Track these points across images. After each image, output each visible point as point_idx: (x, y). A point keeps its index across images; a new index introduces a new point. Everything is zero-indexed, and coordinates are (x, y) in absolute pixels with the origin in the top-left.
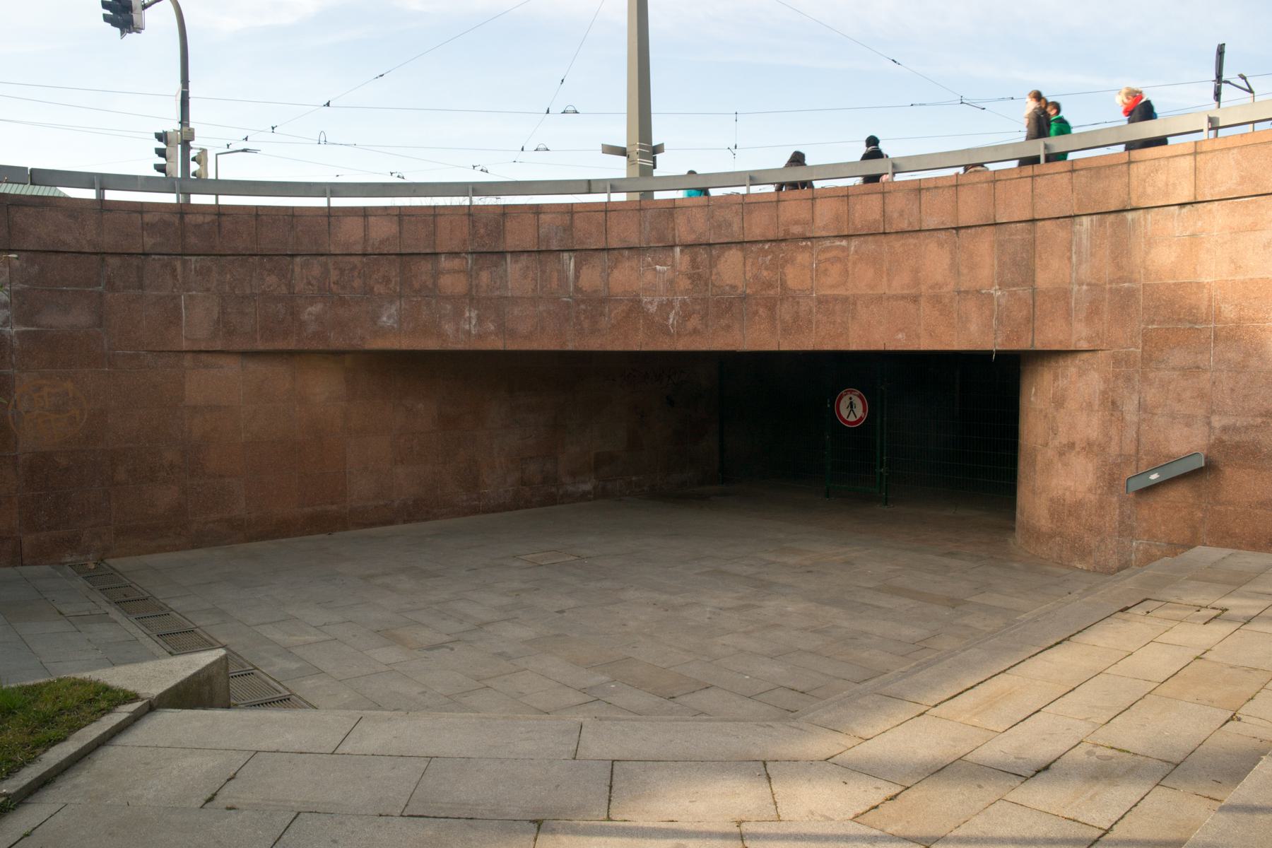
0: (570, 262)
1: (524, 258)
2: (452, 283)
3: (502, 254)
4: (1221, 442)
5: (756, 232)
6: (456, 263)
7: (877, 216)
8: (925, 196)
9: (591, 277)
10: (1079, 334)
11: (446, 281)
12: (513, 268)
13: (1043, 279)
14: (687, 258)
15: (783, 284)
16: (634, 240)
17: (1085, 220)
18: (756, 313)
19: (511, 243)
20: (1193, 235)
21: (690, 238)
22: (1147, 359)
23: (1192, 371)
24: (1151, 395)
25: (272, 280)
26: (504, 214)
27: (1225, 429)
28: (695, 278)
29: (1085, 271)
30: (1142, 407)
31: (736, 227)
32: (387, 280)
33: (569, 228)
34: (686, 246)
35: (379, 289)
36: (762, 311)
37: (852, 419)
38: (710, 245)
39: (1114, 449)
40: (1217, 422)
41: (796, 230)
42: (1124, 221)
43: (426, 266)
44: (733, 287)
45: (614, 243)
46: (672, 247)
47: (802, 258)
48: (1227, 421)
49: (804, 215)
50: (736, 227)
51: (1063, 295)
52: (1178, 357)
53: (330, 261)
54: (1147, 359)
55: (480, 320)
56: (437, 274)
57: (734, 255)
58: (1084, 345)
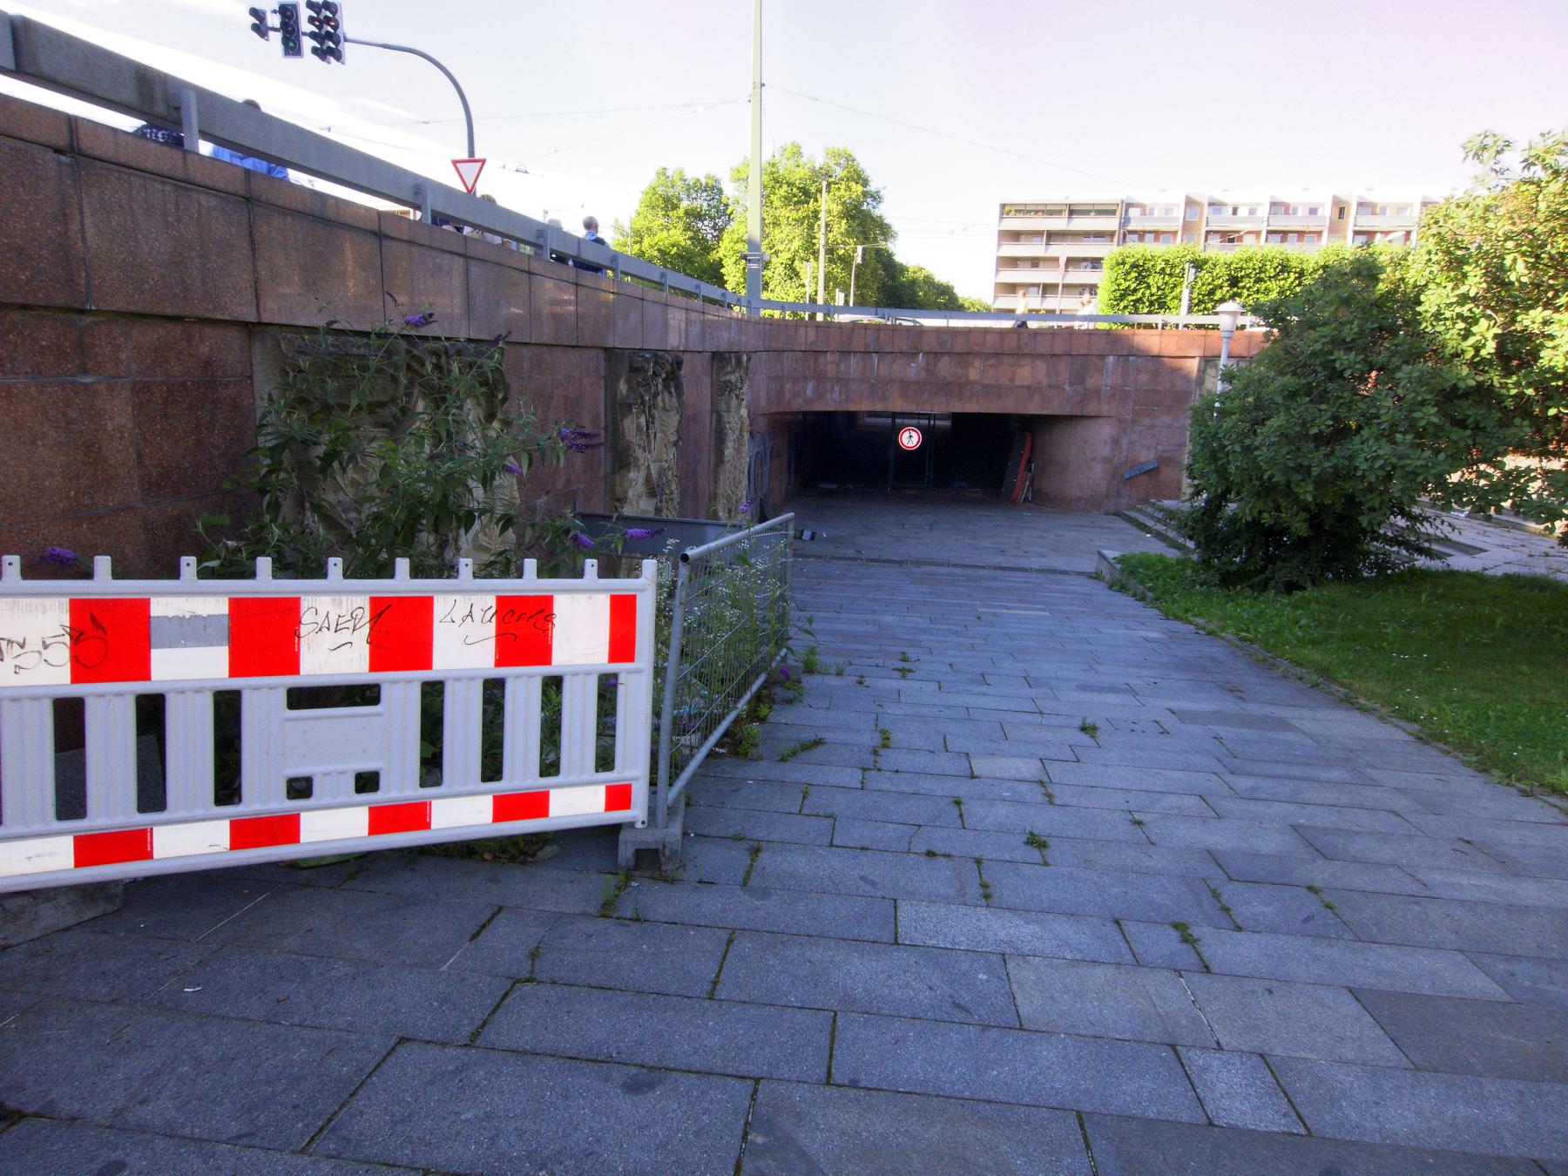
0: (875, 358)
1: (858, 355)
2: (831, 370)
3: (849, 352)
4: (1160, 456)
5: (958, 349)
7: (1015, 344)
8: (1038, 337)
10: (1105, 408)
11: (829, 367)
12: (853, 360)
13: (1090, 383)
14: (925, 360)
16: (904, 348)
19: (855, 347)
20: (1157, 370)
21: (928, 349)
22: (1133, 422)
23: (1151, 427)
24: (1134, 437)
26: (853, 329)
27: (1163, 451)
28: (927, 370)
29: (1109, 381)
30: (1130, 442)
31: (949, 344)
33: (878, 339)
34: (926, 353)
37: (910, 445)
38: (936, 353)
39: (1116, 460)
40: (1160, 448)
41: (977, 349)
42: (1128, 361)
45: (896, 350)
46: (917, 354)
47: (977, 363)
50: (949, 344)
51: (1098, 392)
52: (1147, 421)
54: (1133, 422)
55: (840, 393)
57: (945, 360)
58: (1105, 414)
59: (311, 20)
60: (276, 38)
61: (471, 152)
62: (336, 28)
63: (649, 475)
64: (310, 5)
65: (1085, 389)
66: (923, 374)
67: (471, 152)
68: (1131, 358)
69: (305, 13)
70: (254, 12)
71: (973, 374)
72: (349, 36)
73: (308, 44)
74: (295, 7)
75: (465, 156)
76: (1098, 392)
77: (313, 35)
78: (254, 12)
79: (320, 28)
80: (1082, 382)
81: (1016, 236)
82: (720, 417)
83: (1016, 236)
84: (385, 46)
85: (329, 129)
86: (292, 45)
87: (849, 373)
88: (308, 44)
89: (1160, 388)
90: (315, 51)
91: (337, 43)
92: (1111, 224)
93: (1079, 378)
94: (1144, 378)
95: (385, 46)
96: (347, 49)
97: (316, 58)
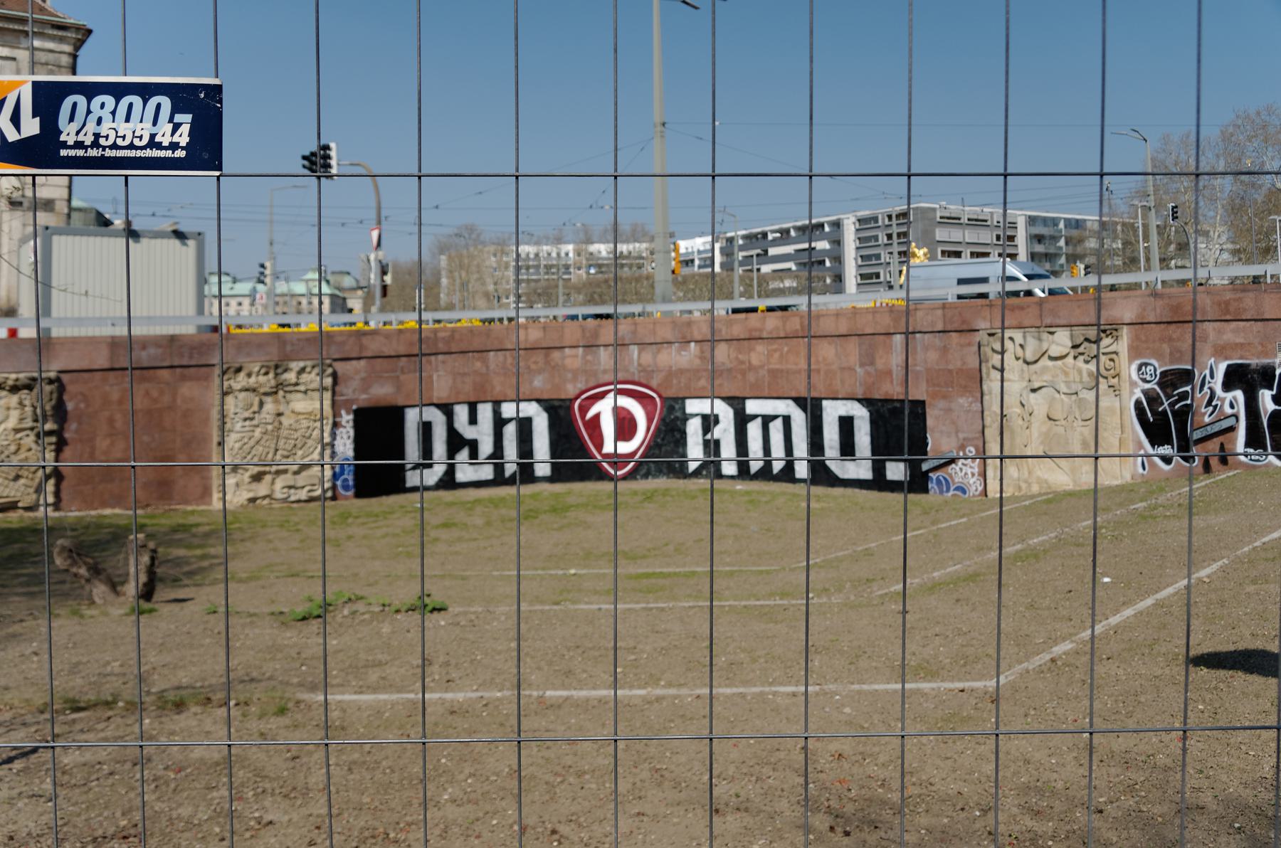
0: (635, 350)
6: (573, 351)
7: (798, 327)
9: (647, 358)
13: (880, 364)
14: (698, 348)
15: (750, 362)
17: (898, 336)
18: (735, 377)
19: (602, 341)
21: (699, 338)
25: (478, 364)
27: (964, 439)
31: (724, 333)
32: (536, 363)
34: (696, 342)
35: (533, 367)
36: (739, 376)
40: (961, 436)
43: (556, 355)
44: (723, 364)
46: (689, 342)
48: (965, 435)
49: (758, 325)
53: (508, 353)
56: (564, 358)
65: (876, 370)
66: (697, 362)
68: (918, 335)
71: (755, 359)
76: (889, 373)
80: (872, 363)
87: (599, 364)
89: (951, 367)
93: (868, 359)
94: (933, 356)
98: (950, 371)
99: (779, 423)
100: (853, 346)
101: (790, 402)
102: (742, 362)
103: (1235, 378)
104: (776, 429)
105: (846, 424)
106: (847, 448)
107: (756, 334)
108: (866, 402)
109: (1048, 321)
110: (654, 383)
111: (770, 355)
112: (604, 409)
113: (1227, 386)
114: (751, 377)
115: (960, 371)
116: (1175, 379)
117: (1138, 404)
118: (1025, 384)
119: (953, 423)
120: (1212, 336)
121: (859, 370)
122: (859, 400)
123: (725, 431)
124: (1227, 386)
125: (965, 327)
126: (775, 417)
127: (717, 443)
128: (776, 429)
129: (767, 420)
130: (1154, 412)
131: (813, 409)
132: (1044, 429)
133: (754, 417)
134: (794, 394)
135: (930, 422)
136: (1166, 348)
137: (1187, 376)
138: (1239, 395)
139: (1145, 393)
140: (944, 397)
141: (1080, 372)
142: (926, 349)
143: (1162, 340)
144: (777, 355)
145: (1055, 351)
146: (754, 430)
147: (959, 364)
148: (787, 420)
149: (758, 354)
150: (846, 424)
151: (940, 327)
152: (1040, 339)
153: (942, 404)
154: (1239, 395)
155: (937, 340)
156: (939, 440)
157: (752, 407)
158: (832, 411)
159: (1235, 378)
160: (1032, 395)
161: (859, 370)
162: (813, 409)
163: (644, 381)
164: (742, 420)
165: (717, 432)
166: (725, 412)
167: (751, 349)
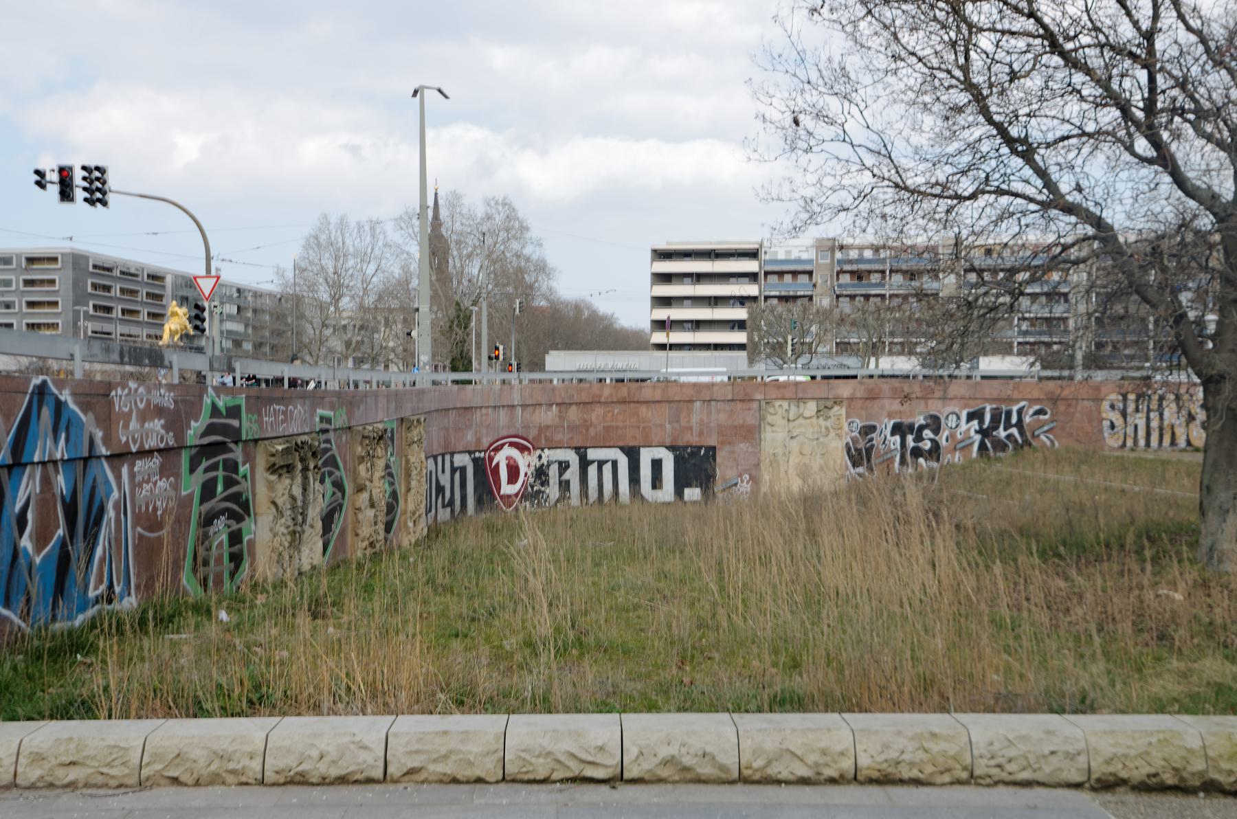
7: (626, 394)
21: (559, 401)
34: (557, 404)
57: (574, 408)
59: (84, 179)
60: (54, 190)
61: (208, 270)
62: (104, 183)
63: (371, 495)
64: (84, 168)
67: (208, 270)
69: (78, 175)
70: (37, 172)
72: (112, 188)
73: (80, 194)
74: (71, 169)
75: (203, 273)
76: (691, 428)
77: (85, 189)
78: (37, 172)
79: (91, 183)
80: (678, 421)
81: (666, 278)
82: (407, 461)
83: (666, 278)
84: (141, 196)
85: (71, 239)
86: (66, 194)
88: (80, 194)
89: (735, 424)
90: (86, 200)
91: (104, 193)
92: (750, 266)
95: (141, 196)
96: (110, 197)
97: (86, 205)
98: (736, 427)
99: (609, 465)
100: (665, 409)
101: (618, 450)
102: (586, 421)
103: (898, 429)
104: (607, 469)
105: (657, 465)
106: (657, 482)
107: (597, 399)
108: (671, 448)
109: (800, 395)
110: (530, 438)
111: (605, 415)
112: (501, 458)
113: (893, 434)
114: (592, 432)
115: (742, 426)
116: (868, 430)
117: (847, 444)
118: (786, 434)
119: (735, 460)
120: (887, 407)
121: (668, 426)
122: (667, 448)
123: (573, 474)
124: (893, 434)
125: (747, 398)
126: (606, 462)
127: (568, 482)
128: (607, 469)
129: (601, 464)
130: (856, 450)
131: (633, 454)
132: (797, 461)
133: (593, 462)
134: (621, 444)
135: (718, 460)
136: (864, 412)
137: (873, 429)
138: (897, 438)
139: (852, 439)
140: (730, 443)
141: (820, 427)
142: (719, 411)
143: (862, 408)
144: (610, 415)
145: (807, 414)
146: (592, 470)
147: (741, 422)
148: (615, 464)
149: (597, 414)
150: (657, 465)
151: (730, 397)
152: (798, 407)
153: (727, 448)
154: (897, 438)
155: (728, 407)
156: (724, 469)
157: (592, 454)
158: (646, 456)
159: (898, 429)
160: (792, 441)
161: (668, 426)
162: (633, 454)
163: (524, 435)
164: (584, 463)
165: (566, 476)
166: (572, 457)
167: (593, 410)
